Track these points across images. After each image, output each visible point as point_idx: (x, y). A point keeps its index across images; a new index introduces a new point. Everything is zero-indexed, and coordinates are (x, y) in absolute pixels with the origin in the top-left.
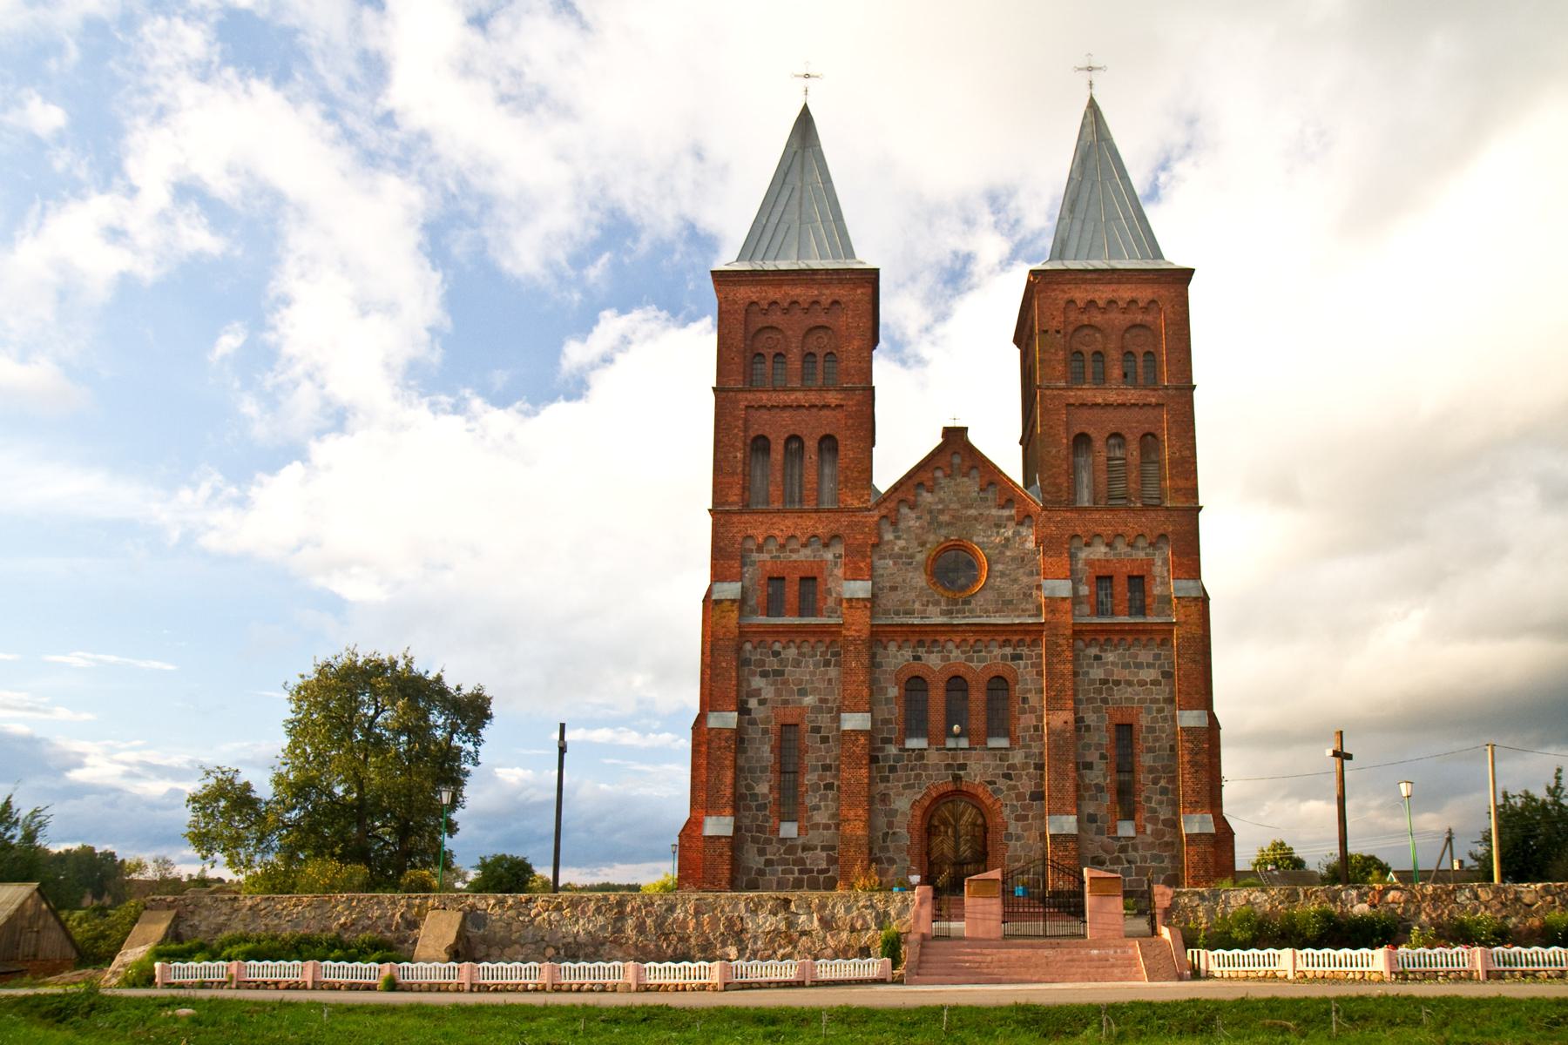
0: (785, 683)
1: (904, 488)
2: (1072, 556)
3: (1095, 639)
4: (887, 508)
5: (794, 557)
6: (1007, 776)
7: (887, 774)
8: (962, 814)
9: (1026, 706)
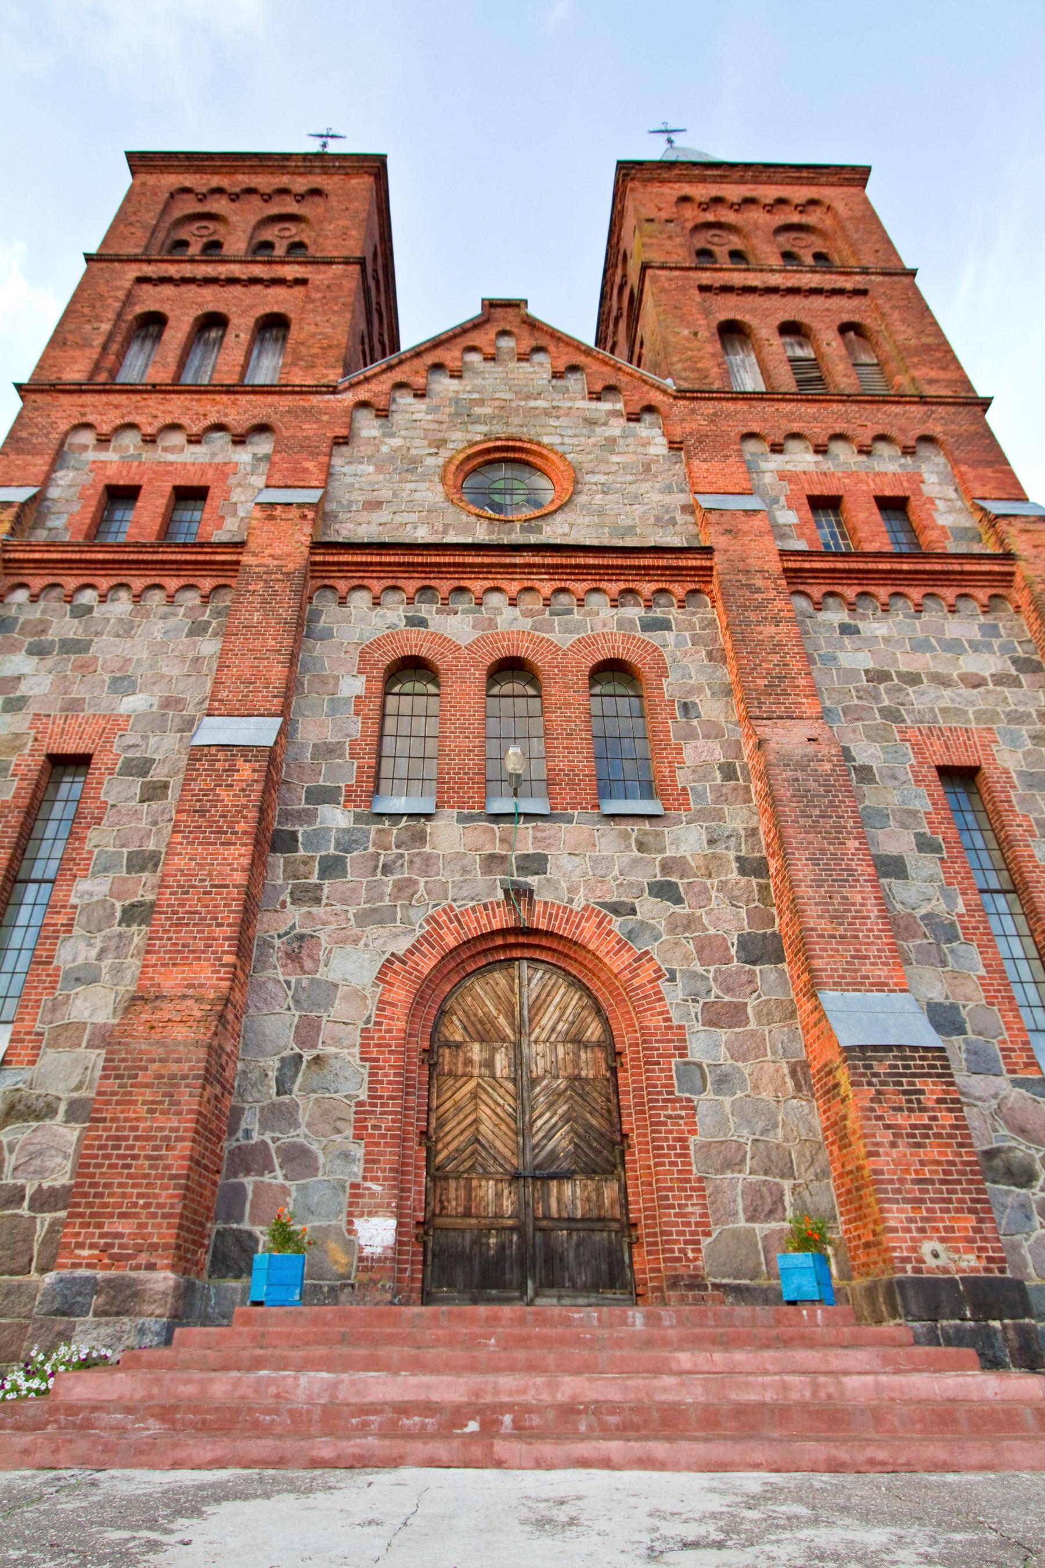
0: (86, 668)
1: (406, 367)
2: (750, 469)
3: (831, 594)
4: (369, 391)
5: (170, 457)
6: (665, 891)
7: (314, 880)
8: (538, 1006)
9: (695, 722)
